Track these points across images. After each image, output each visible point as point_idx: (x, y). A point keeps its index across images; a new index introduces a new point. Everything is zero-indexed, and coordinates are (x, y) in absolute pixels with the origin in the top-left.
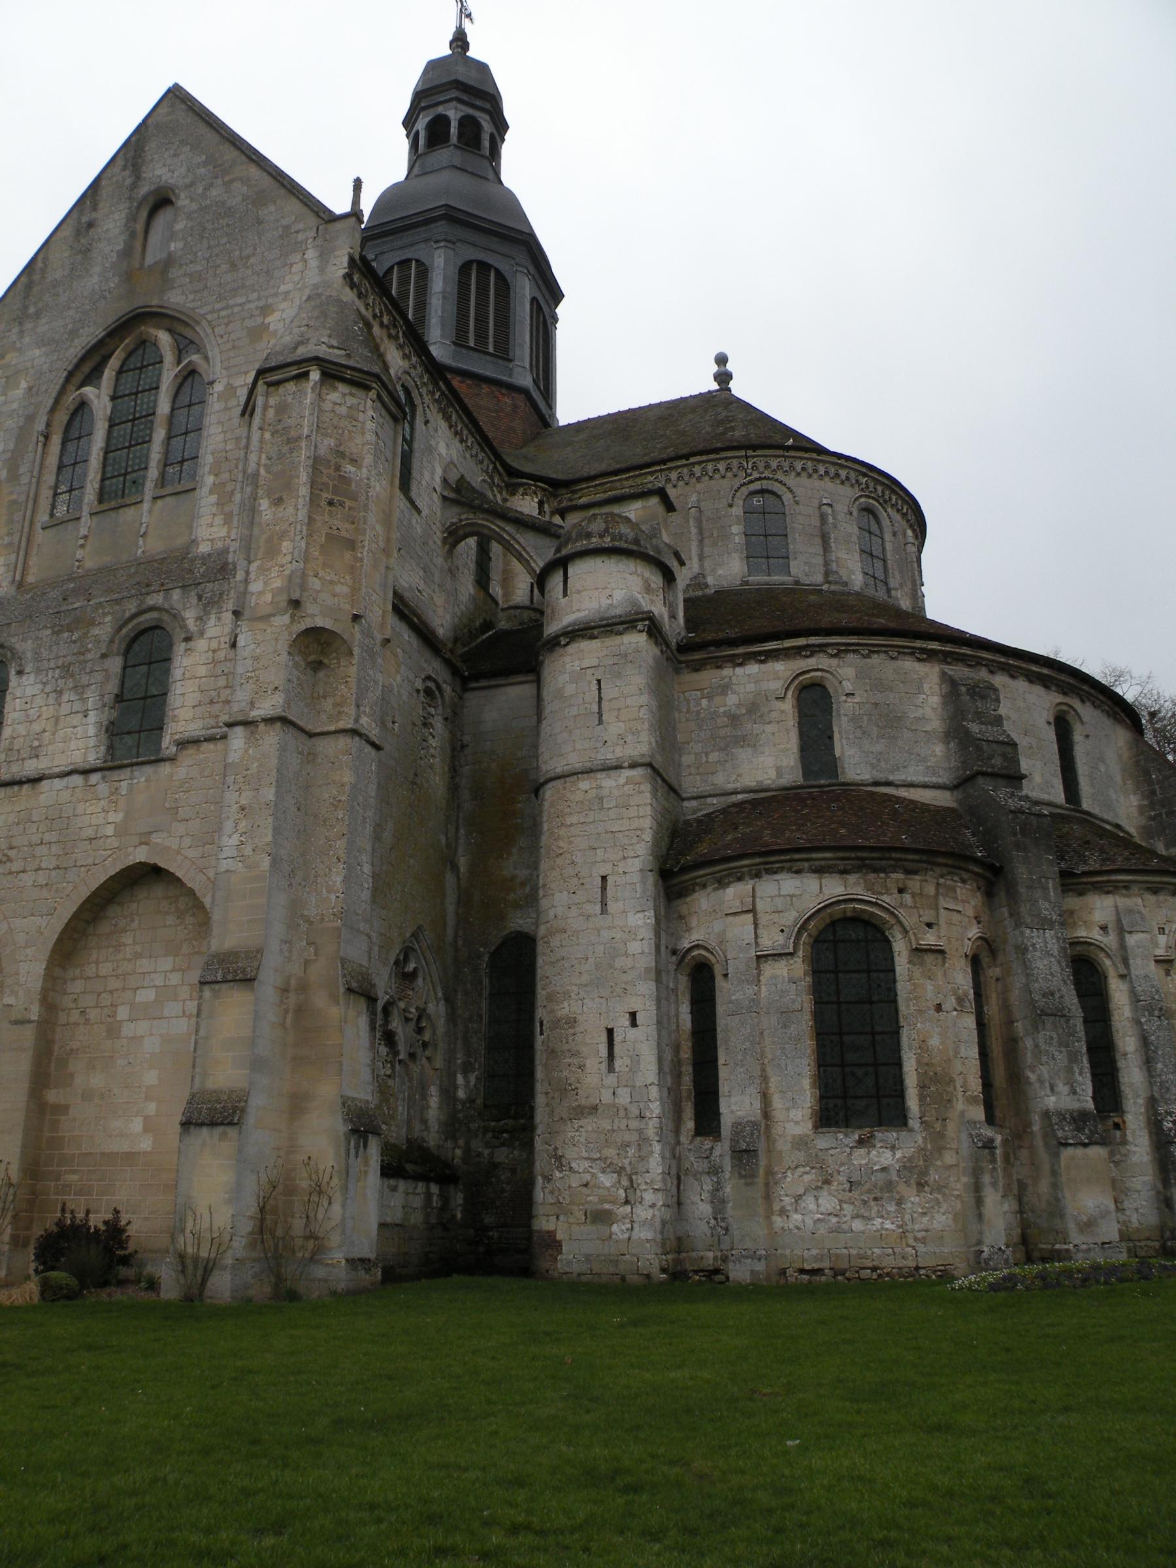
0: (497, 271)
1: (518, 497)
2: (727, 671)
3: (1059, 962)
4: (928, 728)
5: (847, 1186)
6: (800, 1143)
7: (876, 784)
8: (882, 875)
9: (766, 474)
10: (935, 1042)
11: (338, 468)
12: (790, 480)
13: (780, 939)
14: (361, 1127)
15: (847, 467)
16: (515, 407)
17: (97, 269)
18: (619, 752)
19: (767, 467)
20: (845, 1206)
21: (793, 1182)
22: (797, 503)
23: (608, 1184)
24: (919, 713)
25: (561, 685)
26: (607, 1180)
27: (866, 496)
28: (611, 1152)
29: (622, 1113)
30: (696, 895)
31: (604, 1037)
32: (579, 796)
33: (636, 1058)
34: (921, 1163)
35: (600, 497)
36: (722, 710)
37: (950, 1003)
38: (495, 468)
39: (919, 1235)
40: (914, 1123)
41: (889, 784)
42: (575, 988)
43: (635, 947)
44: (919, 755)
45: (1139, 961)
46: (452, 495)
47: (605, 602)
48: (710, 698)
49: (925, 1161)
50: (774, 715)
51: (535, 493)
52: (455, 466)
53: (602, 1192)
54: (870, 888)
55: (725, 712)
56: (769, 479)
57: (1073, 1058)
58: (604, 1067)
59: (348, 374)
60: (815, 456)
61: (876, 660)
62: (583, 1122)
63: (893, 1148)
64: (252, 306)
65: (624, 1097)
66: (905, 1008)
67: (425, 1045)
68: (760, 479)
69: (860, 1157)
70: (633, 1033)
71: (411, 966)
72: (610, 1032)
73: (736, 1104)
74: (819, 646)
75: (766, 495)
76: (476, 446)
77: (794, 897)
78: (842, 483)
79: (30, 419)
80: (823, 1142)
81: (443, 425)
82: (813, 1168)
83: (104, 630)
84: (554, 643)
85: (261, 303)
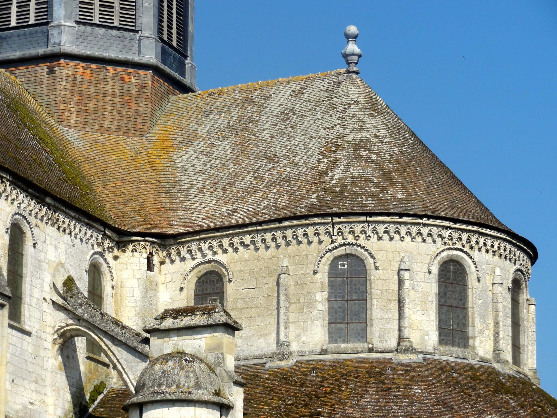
1: (129, 253)
12: (372, 244)
16: (142, 86)
19: (352, 232)
22: (376, 268)
27: (448, 249)
38: (105, 235)
46: (60, 301)
51: (145, 247)
52: (63, 266)
60: (397, 219)
68: (345, 245)
76: (84, 229)
81: (51, 230)
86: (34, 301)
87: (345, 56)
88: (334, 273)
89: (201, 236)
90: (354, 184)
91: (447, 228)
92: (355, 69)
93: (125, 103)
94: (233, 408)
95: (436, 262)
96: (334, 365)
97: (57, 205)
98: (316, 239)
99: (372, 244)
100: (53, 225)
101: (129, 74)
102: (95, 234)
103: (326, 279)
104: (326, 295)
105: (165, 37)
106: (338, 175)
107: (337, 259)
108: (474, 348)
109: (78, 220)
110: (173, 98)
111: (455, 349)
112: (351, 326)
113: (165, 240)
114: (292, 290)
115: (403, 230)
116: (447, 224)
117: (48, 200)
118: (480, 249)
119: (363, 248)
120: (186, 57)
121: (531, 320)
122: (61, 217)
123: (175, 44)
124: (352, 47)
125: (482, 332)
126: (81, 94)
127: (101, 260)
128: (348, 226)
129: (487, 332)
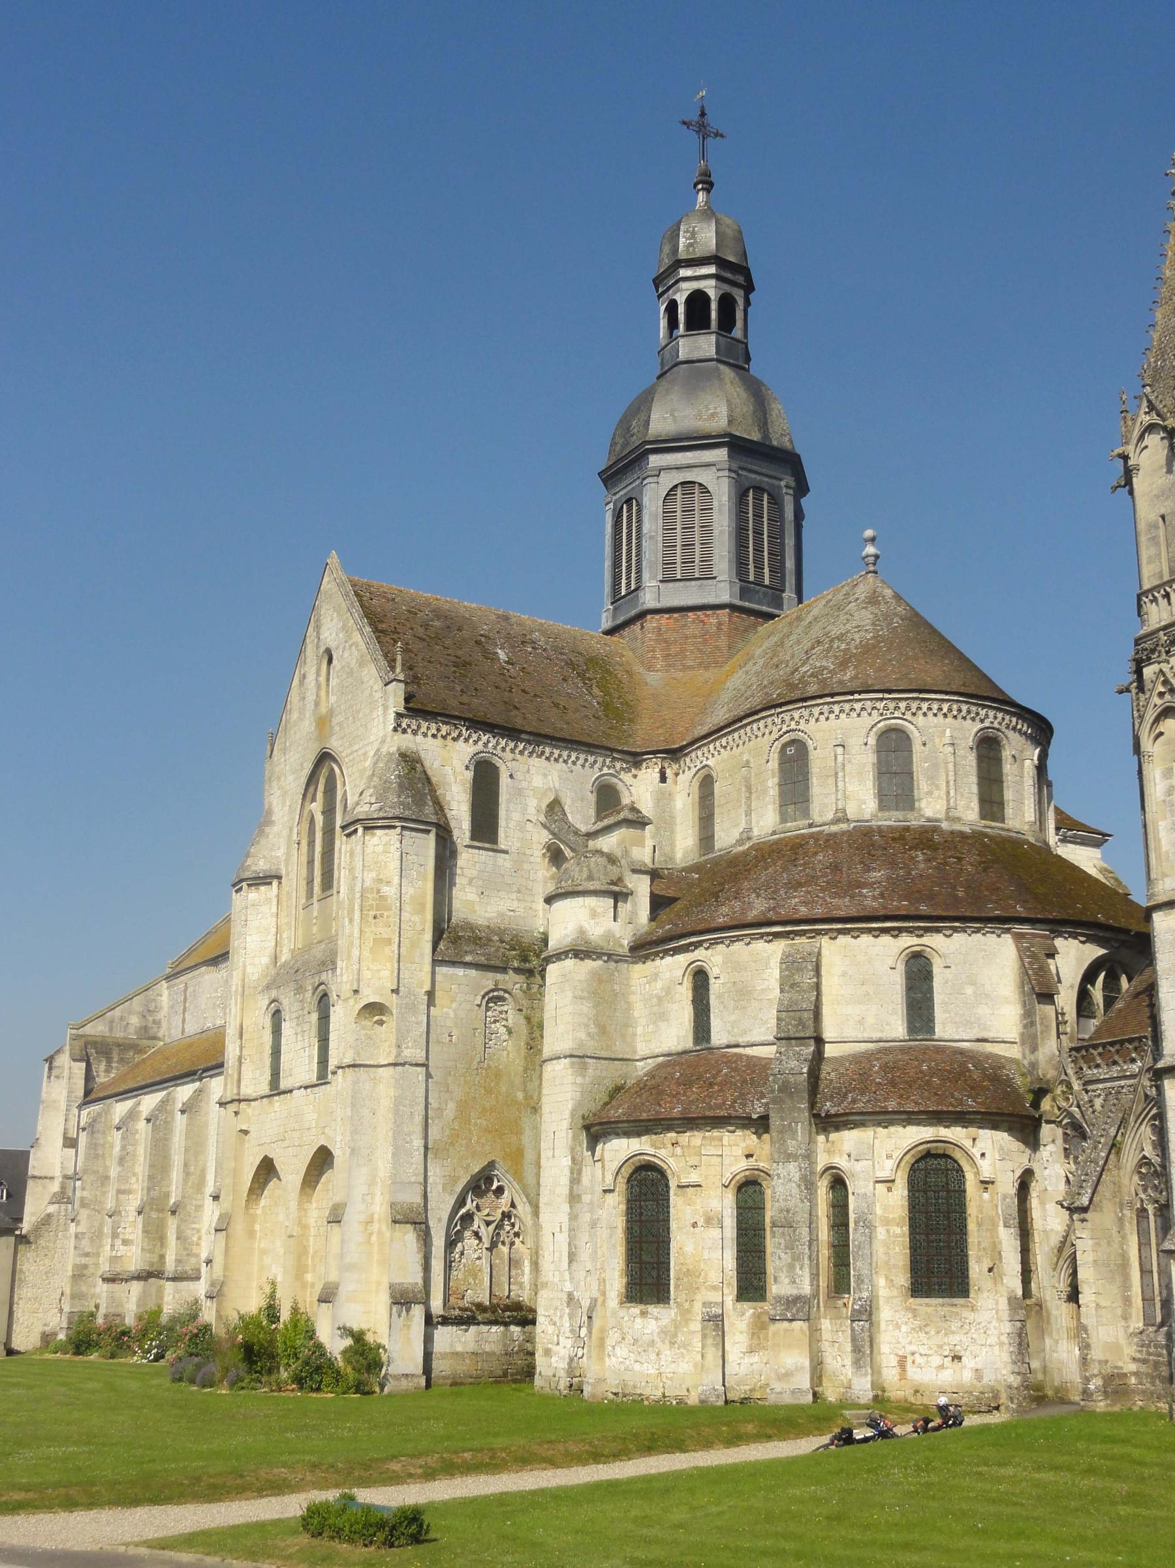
0: (700, 485)
2: (658, 962)
3: (799, 1186)
6: (614, 1313)
7: (729, 1047)
9: (793, 726)
10: (689, 1249)
11: (379, 891)
12: (811, 727)
14: (402, 1300)
15: (860, 700)
16: (720, 624)
17: (308, 715)
19: (792, 719)
21: (613, 1337)
24: (765, 985)
37: (701, 1223)
39: (669, 1375)
45: (862, 1183)
54: (653, 1145)
57: (796, 1258)
59: (380, 823)
60: (829, 699)
61: (738, 946)
63: (657, 1319)
64: (360, 752)
66: (673, 1225)
67: (517, 1235)
68: (788, 732)
71: (495, 1185)
76: (582, 757)
79: (291, 829)
80: (622, 1313)
81: (536, 762)
83: (309, 995)
84: (548, 960)
85: (363, 751)
86: (512, 824)
87: (864, 558)
88: (784, 760)
90: (812, 675)
91: (882, 699)
92: (871, 568)
93: (705, 642)
94: (632, 893)
95: (872, 733)
96: (776, 842)
97: (537, 739)
98: (767, 731)
99: (811, 727)
100: (539, 756)
101: (707, 616)
102: (600, 760)
103: (777, 766)
104: (776, 780)
105: (751, 578)
106: (804, 669)
107: (785, 746)
108: (920, 809)
109: (572, 749)
110: (760, 628)
111: (895, 813)
112: (798, 806)
113: (675, 754)
114: (753, 781)
115: (836, 708)
116: (880, 695)
117: (523, 736)
118: (925, 714)
120: (783, 591)
121: (1026, 775)
122: (548, 750)
123: (767, 582)
124: (870, 550)
125: (930, 793)
126: (666, 641)
127: (615, 780)
128: (789, 714)
129: (936, 793)
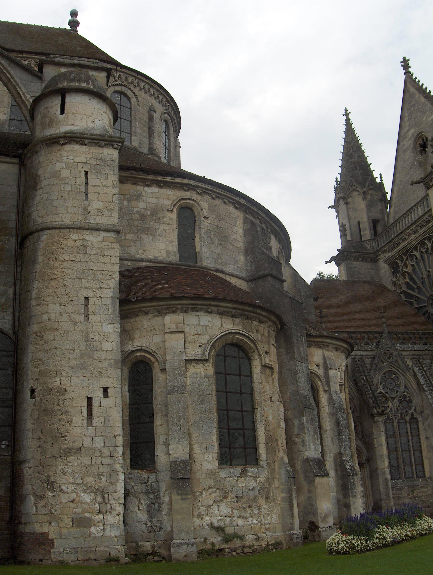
2: (140, 188)
4: (238, 246)
5: (235, 499)
6: (211, 474)
7: (217, 271)
8: (250, 321)
13: (199, 351)
18: (98, 220)
19: (126, 80)
20: (234, 511)
23: (88, 501)
25: (58, 169)
26: (87, 498)
28: (90, 479)
29: (98, 454)
30: (138, 318)
31: (85, 403)
32: (70, 243)
33: (108, 418)
34: (267, 486)
35: (69, 61)
36: (136, 209)
40: (263, 463)
41: (222, 272)
42: (66, 369)
43: (107, 346)
44: (234, 259)
47: (91, 125)
48: (129, 200)
49: (269, 485)
50: (166, 219)
53: (84, 506)
55: (137, 211)
56: (126, 87)
58: (85, 422)
62: (71, 459)
65: (99, 443)
69: (242, 483)
70: (105, 402)
72: (90, 400)
73: (169, 450)
74: (194, 186)
75: (122, 96)
77: (206, 327)
78: (159, 102)
80: (222, 474)
82: (217, 489)
89: (24, 56)
119: (132, 91)
